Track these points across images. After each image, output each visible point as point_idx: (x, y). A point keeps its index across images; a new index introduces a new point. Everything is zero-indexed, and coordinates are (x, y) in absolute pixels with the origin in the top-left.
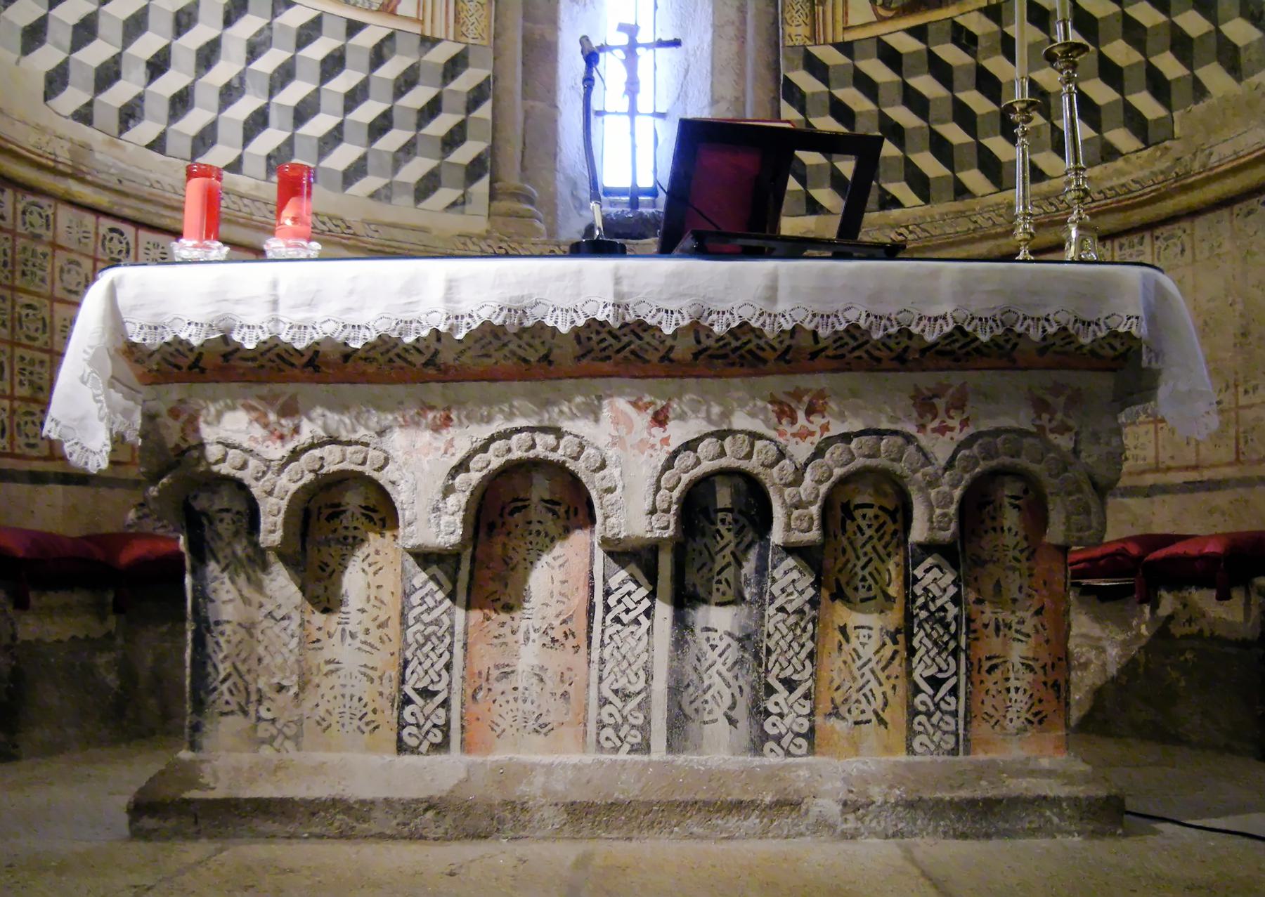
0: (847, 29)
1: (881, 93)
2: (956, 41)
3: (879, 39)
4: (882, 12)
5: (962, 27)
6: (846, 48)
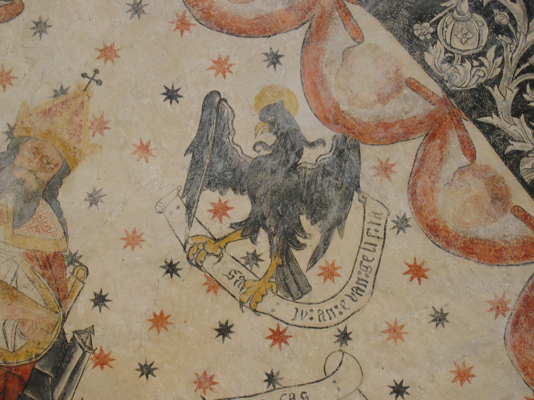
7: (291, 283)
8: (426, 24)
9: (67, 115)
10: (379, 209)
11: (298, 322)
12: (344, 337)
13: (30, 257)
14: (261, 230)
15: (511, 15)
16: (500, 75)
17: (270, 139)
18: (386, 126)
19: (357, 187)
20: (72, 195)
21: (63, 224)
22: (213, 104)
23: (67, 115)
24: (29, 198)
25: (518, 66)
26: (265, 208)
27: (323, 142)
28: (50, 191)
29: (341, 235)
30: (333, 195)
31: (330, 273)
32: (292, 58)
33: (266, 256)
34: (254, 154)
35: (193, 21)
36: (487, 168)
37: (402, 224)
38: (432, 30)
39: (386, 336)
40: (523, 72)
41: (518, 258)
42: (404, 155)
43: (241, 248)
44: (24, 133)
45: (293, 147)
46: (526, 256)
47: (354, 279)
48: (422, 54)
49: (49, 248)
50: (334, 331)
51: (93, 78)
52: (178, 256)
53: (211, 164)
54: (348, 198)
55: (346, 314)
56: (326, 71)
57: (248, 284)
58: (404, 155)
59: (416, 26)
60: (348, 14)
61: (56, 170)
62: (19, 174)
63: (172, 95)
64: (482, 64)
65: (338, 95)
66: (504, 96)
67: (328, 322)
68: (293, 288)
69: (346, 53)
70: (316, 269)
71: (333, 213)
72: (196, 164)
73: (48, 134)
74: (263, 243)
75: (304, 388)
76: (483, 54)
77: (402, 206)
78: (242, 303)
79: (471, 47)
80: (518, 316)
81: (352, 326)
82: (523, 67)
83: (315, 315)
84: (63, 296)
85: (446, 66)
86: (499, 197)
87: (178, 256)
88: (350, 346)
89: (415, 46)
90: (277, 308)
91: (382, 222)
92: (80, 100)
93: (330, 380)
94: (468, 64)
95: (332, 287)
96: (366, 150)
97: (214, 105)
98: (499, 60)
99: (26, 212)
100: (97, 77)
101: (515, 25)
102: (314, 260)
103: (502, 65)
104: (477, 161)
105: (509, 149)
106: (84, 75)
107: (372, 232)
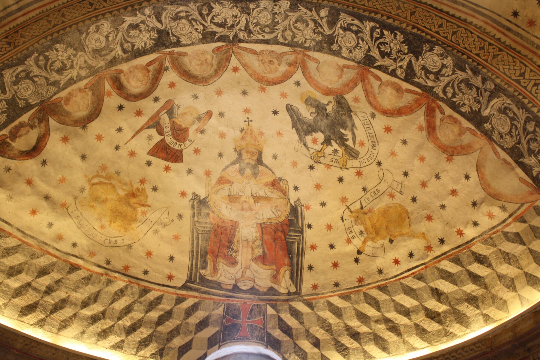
7: (352, 154)
8: (334, 44)
9: (249, 136)
10: (363, 114)
11: (362, 166)
12: (379, 164)
13: (267, 185)
14: (332, 141)
15: (356, 25)
16: (369, 47)
17: (314, 110)
18: (348, 85)
19: (351, 111)
20: (267, 159)
21: (270, 170)
22: (289, 109)
23: (249, 136)
24: (254, 167)
25: (372, 41)
26: (328, 133)
27: (330, 102)
28: (260, 161)
29: (357, 129)
30: (344, 117)
31: (362, 144)
32: (303, 81)
33: (338, 149)
34: (312, 118)
35: (265, 86)
36: (387, 81)
37: (373, 116)
38: (337, 45)
39: (392, 157)
40: (375, 42)
41: (417, 107)
42: (359, 91)
43: (329, 150)
44: (240, 148)
45: (323, 109)
46: (419, 105)
47: (370, 142)
48: (341, 55)
49: (270, 179)
50: (375, 163)
51: (248, 121)
52: (312, 163)
53: (302, 128)
54: (350, 116)
55: (375, 155)
56: (316, 78)
57: (339, 160)
58: (359, 91)
59: (332, 47)
60: (309, 56)
61: (257, 154)
62: (246, 161)
63: (275, 113)
64: (361, 47)
65: (326, 84)
66: (375, 53)
67: (371, 161)
68: (354, 154)
69: (317, 69)
70: (357, 145)
71: (349, 124)
72: (298, 131)
73: (247, 144)
74: (335, 146)
75: (376, 188)
76: (358, 43)
77: (370, 110)
78: (341, 168)
79: (353, 43)
80: (428, 129)
81: (379, 159)
82: (374, 40)
83: (366, 160)
84: (285, 193)
85: (351, 54)
86: (398, 89)
87: (312, 163)
88: (384, 166)
89: (337, 53)
90: (353, 164)
91: (367, 118)
92: (249, 130)
93: (383, 181)
94: (357, 50)
95: (366, 148)
96: (346, 96)
97: (289, 109)
98: (365, 42)
99: (256, 172)
100: (249, 120)
101: (360, 28)
102: (354, 143)
103: (367, 44)
104: (383, 81)
105: (390, 70)
106: (245, 121)
107: (366, 123)
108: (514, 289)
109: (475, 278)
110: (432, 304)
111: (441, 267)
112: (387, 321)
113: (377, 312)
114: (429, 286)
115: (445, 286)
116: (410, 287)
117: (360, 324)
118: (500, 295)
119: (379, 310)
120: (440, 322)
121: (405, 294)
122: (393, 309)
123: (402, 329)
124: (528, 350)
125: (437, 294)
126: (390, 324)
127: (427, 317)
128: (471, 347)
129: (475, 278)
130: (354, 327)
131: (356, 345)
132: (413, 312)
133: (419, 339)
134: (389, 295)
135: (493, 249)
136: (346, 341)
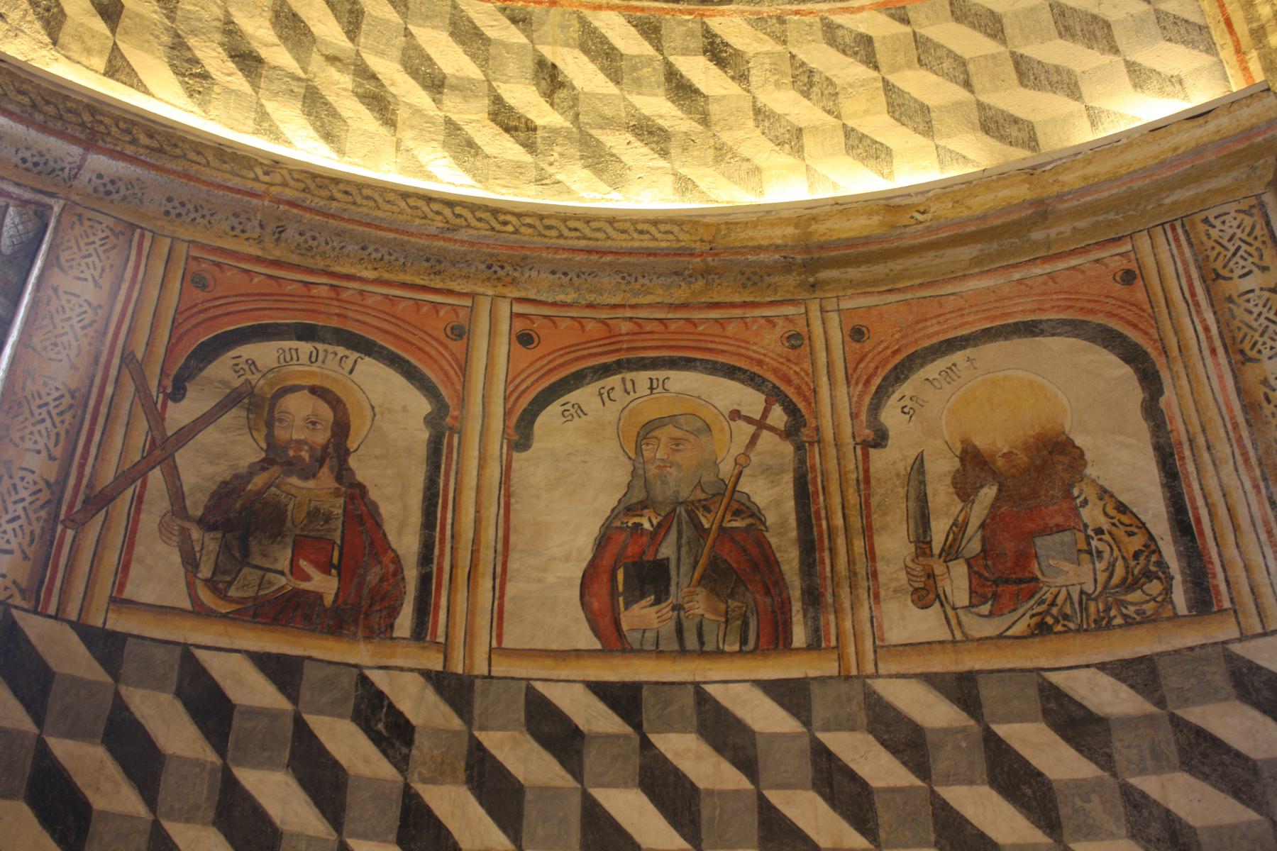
0: (119, 602)
1: (169, 781)
2: (363, 719)
3: (187, 653)
4: (206, 596)
5: (381, 695)
6: (107, 646)
108: (798, 151)
109: (681, 89)
110: (524, 97)
111: (596, 24)
112: (364, 73)
113: (344, 37)
114: (535, 50)
115: (581, 71)
116: (476, 27)
117: (276, 41)
118: (745, 150)
119: (352, 31)
120: (530, 147)
121: (452, 34)
122: (397, 53)
123: (402, 114)
124: (813, 286)
125: (550, 79)
126: (370, 86)
127: (493, 120)
128: (645, 227)
129: (681, 89)
130: (252, 36)
131: (239, 82)
132: (453, 88)
133: (450, 159)
134: (404, 16)
135: (770, 46)
136: (212, 57)
